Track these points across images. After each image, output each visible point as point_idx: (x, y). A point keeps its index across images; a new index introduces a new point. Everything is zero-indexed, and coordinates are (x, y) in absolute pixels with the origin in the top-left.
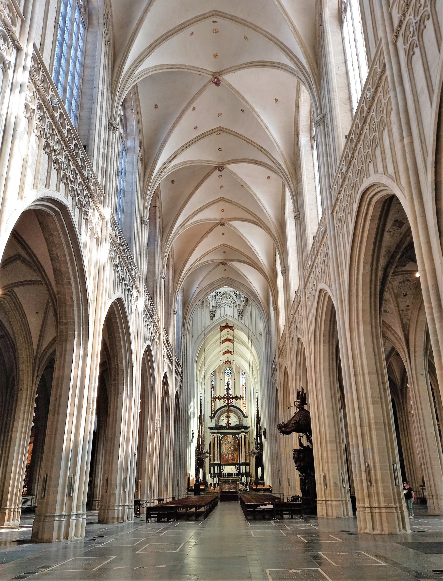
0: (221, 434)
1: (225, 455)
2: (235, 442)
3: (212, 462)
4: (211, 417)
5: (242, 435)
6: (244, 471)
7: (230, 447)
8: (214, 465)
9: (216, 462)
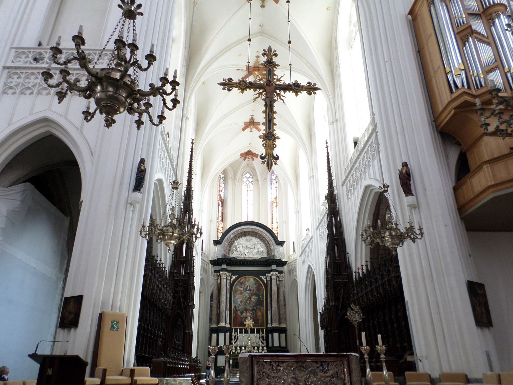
0: (233, 273)
1: (239, 313)
2: (259, 288)
3: (214, 326)
4: (216, 243)
5: (273, 275)
6: (276, 344)
7: (250, 298)
8: (217, 331)
9: (222, 324)
